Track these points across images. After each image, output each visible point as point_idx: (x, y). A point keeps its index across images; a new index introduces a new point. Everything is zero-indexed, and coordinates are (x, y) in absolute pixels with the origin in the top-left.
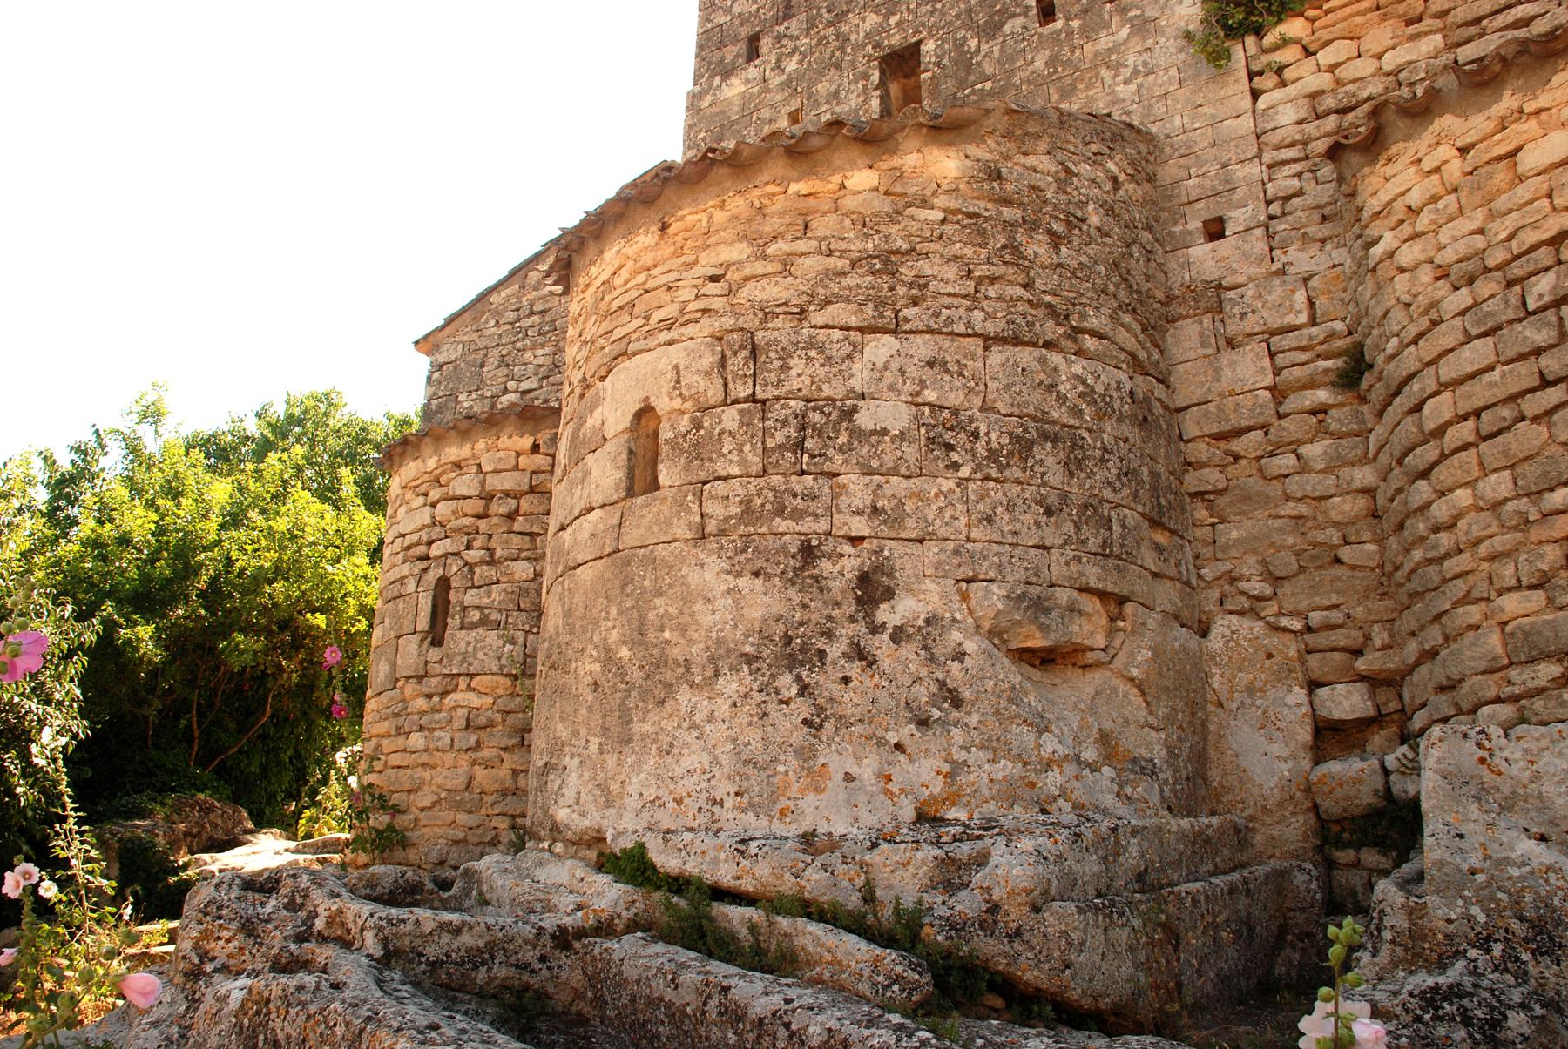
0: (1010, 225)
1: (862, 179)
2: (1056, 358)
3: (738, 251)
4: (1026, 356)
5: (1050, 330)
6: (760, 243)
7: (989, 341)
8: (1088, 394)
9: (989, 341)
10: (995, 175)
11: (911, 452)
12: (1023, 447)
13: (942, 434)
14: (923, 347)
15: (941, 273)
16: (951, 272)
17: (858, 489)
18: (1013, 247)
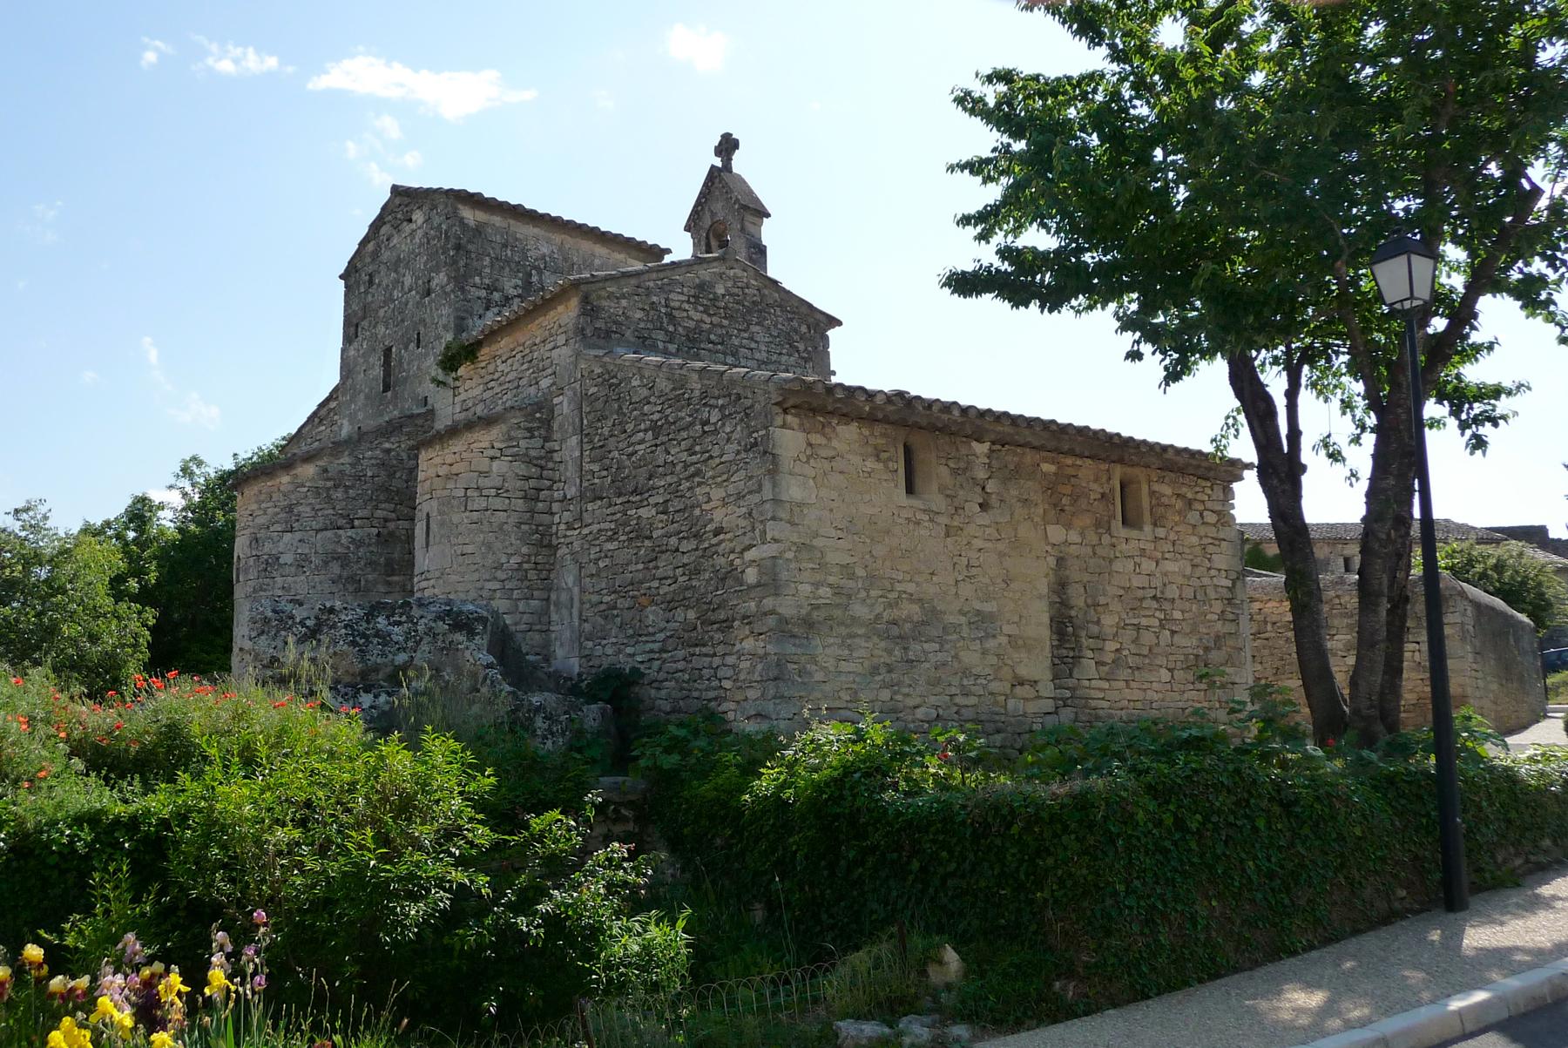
0: (328, 489)
1: (285, 479)
2: (341, 532)
3: (254, 507)
4: (329, 534)
5: (342, 522)
6: (259, 502)
7: (317, 531)
8: (353, 541)
9: (317, 531)
10: (325, 471)
11: (293, 569)
12: (326, 563)
13: (301, 563)
14: (298, 535)
15: (305, 510)
16: (308, 509)
17: (279, 580)
18: (328, 496)
